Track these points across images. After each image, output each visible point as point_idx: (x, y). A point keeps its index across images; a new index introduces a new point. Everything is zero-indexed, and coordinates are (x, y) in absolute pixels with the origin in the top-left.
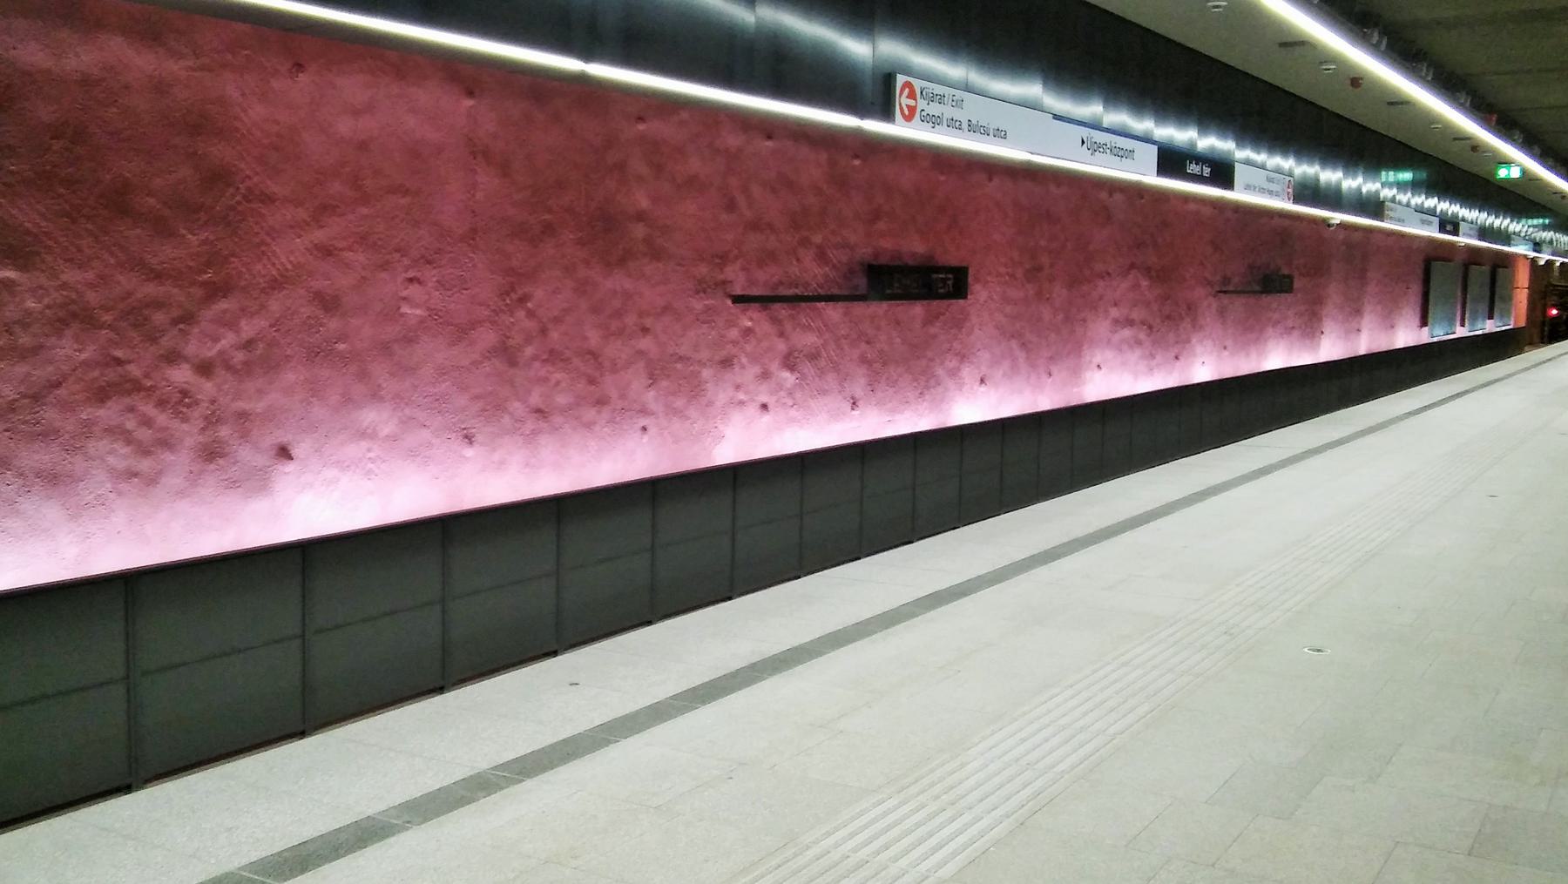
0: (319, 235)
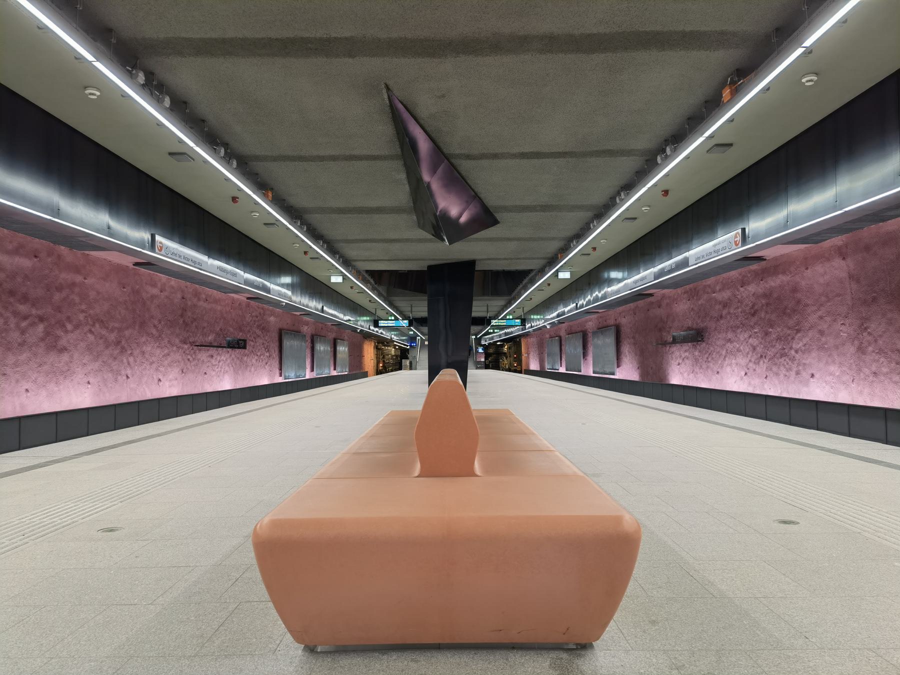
0: (820, 313)
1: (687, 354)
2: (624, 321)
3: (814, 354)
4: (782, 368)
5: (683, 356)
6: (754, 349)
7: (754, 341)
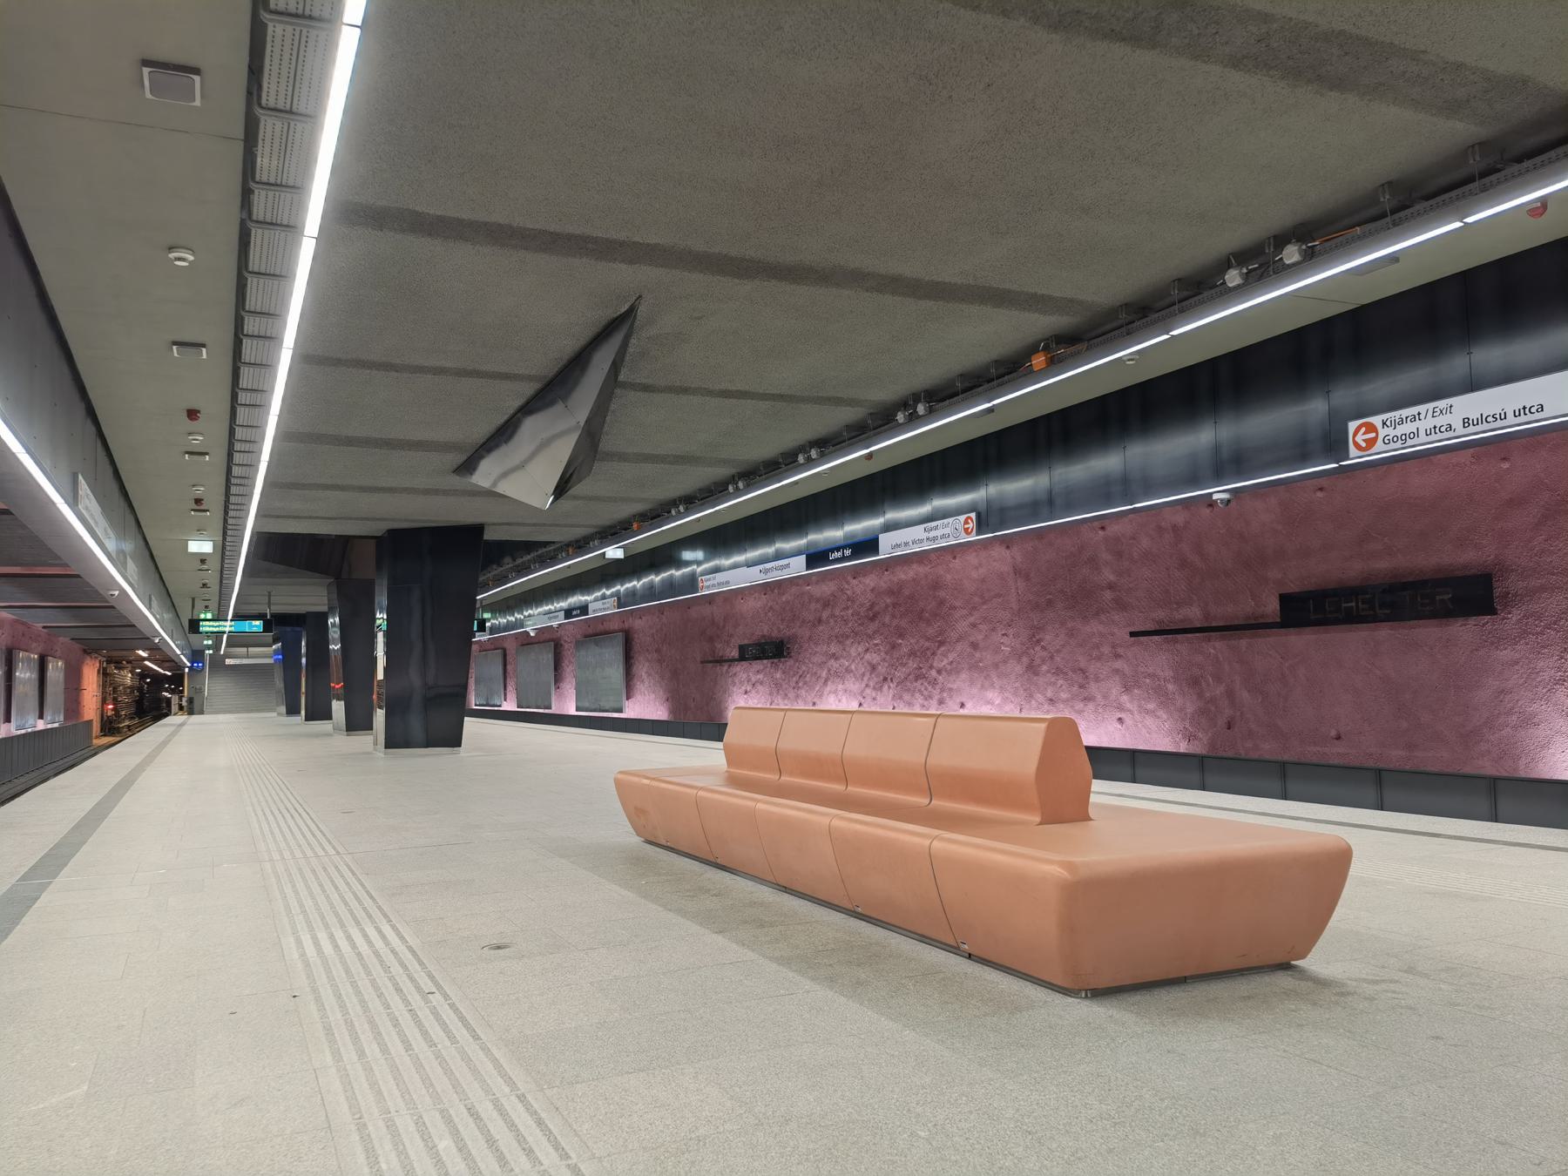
0: (972, 619)
1: (760, 676)
2: (638, 624)
3: (963, 676)
4: (917, 695)
5: (753, 679)
6: (874, 668)
7: (873, 657)
